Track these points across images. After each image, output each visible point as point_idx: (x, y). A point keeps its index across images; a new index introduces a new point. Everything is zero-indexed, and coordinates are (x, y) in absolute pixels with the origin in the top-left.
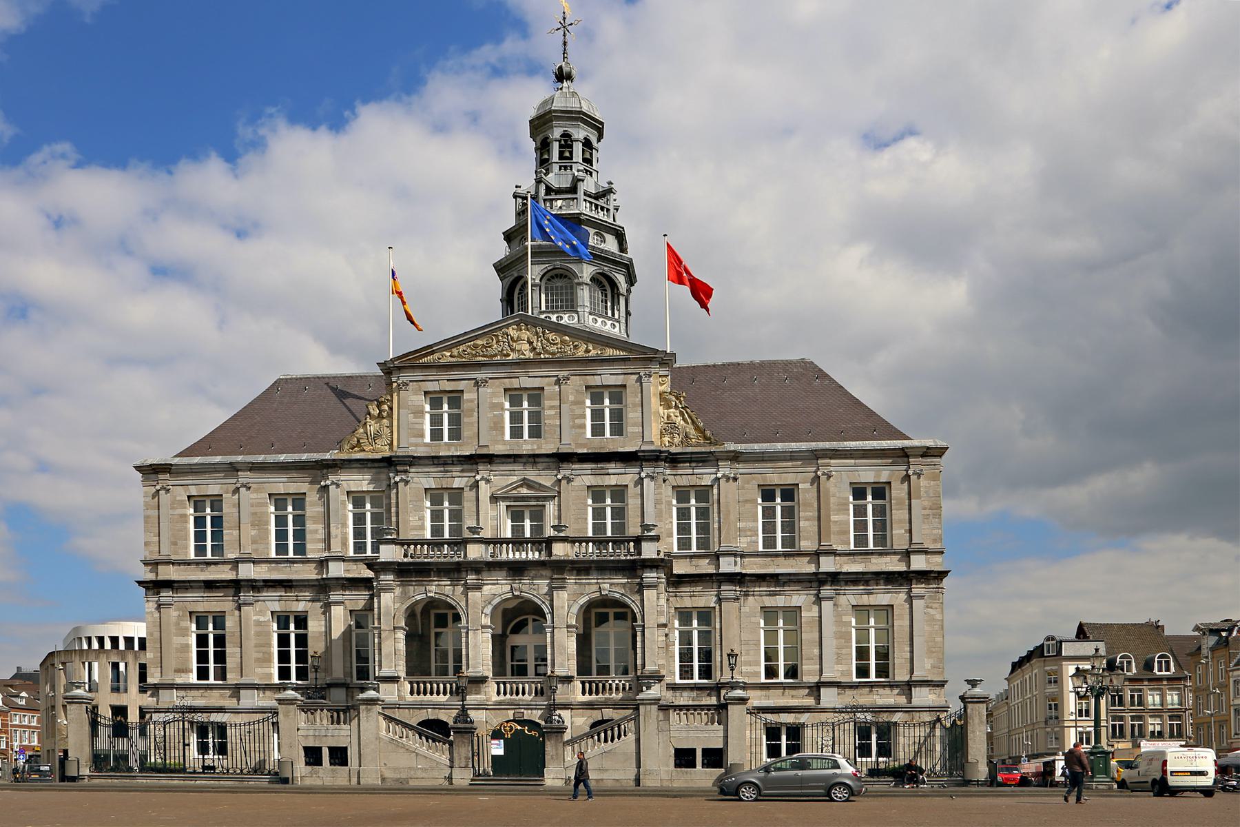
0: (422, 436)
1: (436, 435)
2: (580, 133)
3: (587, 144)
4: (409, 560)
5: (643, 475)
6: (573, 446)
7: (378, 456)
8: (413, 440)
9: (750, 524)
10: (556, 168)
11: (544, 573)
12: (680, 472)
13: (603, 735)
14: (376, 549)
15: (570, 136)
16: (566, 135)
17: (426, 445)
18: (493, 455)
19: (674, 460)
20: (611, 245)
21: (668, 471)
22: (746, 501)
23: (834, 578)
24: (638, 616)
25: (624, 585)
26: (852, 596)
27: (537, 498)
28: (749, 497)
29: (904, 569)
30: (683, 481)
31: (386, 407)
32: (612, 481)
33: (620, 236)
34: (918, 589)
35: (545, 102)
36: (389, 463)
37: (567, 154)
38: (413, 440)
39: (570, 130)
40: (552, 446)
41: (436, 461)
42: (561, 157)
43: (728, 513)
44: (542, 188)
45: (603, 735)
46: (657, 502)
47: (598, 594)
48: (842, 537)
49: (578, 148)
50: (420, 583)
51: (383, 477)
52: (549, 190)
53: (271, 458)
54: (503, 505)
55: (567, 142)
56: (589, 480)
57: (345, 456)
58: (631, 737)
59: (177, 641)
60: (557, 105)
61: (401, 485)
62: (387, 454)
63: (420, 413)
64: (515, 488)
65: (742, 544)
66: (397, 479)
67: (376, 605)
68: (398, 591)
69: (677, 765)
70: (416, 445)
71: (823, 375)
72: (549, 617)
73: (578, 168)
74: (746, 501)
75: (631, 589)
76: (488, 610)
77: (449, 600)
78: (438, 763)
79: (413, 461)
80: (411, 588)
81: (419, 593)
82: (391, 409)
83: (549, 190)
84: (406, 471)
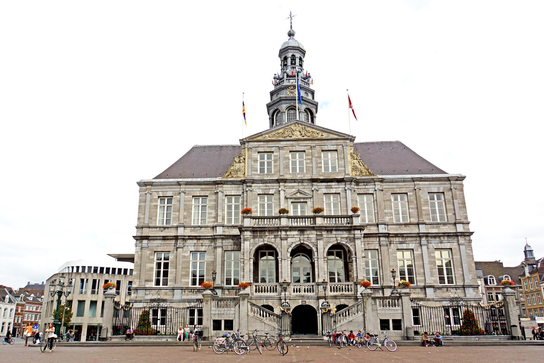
0: (257, 171)
1: (262, 170)
2: (298, 55)
3: (300, 59)
4: (256, 226)
5: (346, 188)
6: (318, 175)
7: (239, 179)
8: (253, 173)
9: (390, 211)
10: (290, 67)
11: (313, 232)
12: (360, 187)
13: (347, 312)
14: (243, 221)
15: (294, 56)
16: (293, 56)
17: (259, 175)
18: (287, 179)
19: (357, 182)
20: (310, 97)
21: (356, 187)
22: (387, 200)
23: (427, 235)
24: (354, 253)
25: (347, 238)
26: (434, 243)
27: (304, 198)
28: (388, 198)
29: (455, 231)
30: (362, 191)
31: (242, 158)
32: (334, 191)
33: (313, 93)
34: (461, 240)
35: (285, 43)
36: (243, 182)
37: (294, 63)
38: (253, 173)
39: (295, 54)
40: (309, 176)
41: (263, 181)
42: (292, 64)
43: (381, 205)
44: (285, 75)
45: (347, 312)
46: (352, 200)
47: (336, 242)
48: (428, 217)
49: (297, 61)
50: (261, 237)
51: (241, 189)
52: (288, 76)
53: (194, 180)
54: (290, 201)
55: (293, 58)
56: (325, 191)
57: (225, 179)
58: (361, 314)
59: (149, 265)
60: (290, 45)
61: (249, 192)
62: (243, 178)
63: (256, 161)
64: (295, 194)
65: (387, 219)
66: (247, 189)
67: (242, 248)
68: (252, 240)
69: (382, 329)
70: (255, 175)
71: (406, 148)
72: (316, 253)
73: (298, 69)
74: (387, 200)
75: (350, 240)
76: (290, 250)
77: (273, 245)
78: (274, 328)
79: (253, 181)
80: (257, 239)
81: (260, 242)
82: (244, 159)
83: (288, 76)
84: (251, 186)
